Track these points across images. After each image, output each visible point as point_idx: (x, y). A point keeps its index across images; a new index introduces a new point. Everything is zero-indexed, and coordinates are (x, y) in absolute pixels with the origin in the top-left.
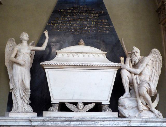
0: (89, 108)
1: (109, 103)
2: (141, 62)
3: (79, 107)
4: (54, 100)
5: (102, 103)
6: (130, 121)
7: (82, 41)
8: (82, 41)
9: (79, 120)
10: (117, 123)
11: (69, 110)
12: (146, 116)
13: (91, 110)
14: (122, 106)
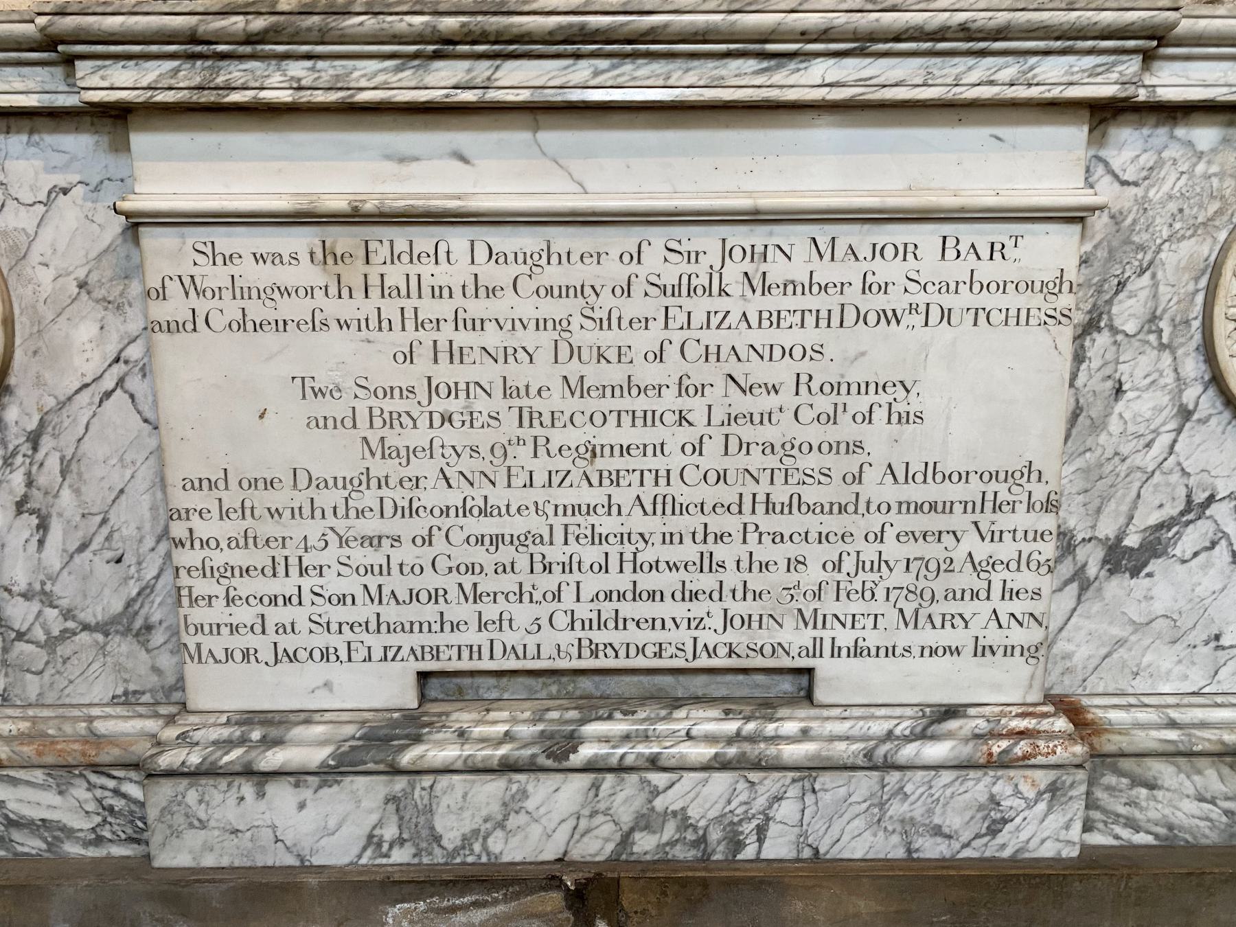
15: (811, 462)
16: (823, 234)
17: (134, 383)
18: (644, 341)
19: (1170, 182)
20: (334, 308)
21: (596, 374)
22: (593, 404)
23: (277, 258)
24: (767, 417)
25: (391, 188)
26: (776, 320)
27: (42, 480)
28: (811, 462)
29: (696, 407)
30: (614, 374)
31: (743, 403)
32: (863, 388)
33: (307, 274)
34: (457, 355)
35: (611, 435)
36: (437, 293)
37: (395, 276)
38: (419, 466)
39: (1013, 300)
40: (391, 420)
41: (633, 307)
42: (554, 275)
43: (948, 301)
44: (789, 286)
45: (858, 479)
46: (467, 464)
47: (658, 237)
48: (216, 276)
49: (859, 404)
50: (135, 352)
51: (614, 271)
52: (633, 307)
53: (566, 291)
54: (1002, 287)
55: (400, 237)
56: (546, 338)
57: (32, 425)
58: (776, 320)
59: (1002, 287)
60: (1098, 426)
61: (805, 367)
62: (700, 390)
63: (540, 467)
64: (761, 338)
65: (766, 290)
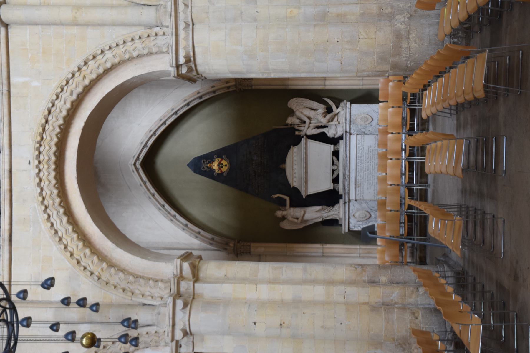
0: (336, 161)
1: (333, 145)
2: (299, 118)
3: (336, 168)
4: (330, 186)
5: (333, 150)
6: (346, 132)
7: (281, 166)
8: (281, 166)
9: (345, 169)
10: (347, 141)
11: (338, 176)
12: (342, 119)
13: (338, 159)
14: (335, 135)
15: (374, 153)
16: (357, 153)
17: (367, 202)
18: (365, 165)
19: (354, 128)
20: (362, 187)
21: (367, 169)
22: (369, 169)
23: (358, 190)
24: (370, 156)
25: (354, 183)
26: (363, 156)
27: (374, 209)
28: (374, 153)
29: (369, 162)
30: (367, 167)
31: (369, 158)
32: (368, 149)
33: (359, 189)
34: (365, 179)
35: (371, 168)
36: (361, 180)
37: (360, 182)
38: (374, 182)
39: (362, 139)
40: (370, 183)
41: (362, 166)
42: (360, 172)
43: (362, 144)
44: (361, 155)
45: (375, 150)
46: (373, 178)
47: (357, 164)
48: (360, 195)
49: (369, 150)
50: (365, 202)
51: (360, 167)
52: (362, 166)
53: (361, 171)
54: (361, 140)
55: (357, 182)
56: (364, 172)
57: (370, 209)
58: (363, 156)
59: (361, 140)
60: (372, 132)
61: (367, 154)
62: (368, 161)
63: (374, 173)
64: (365, 157)
65: (361, 157)
